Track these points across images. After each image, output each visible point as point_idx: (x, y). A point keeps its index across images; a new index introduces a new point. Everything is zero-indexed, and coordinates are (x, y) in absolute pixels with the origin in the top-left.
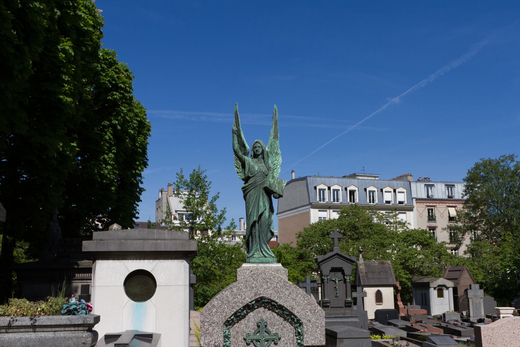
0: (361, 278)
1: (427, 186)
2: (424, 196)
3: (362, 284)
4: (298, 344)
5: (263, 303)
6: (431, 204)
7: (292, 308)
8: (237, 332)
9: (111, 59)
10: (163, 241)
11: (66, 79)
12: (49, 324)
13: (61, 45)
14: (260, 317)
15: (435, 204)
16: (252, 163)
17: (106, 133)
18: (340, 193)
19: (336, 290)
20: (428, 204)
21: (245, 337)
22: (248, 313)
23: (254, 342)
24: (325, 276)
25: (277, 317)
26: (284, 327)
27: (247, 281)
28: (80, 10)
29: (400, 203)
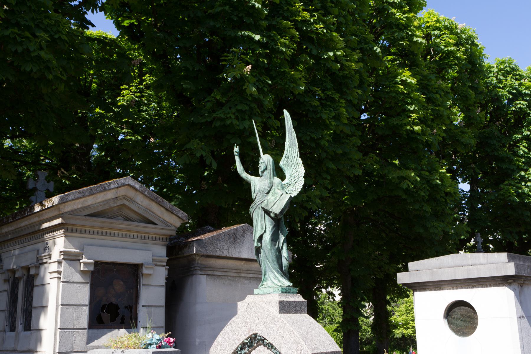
7: (280, 347)
9: (506, 67)
10: (475, 267)
11: (412, 109)
17: (519, 147)
28: (417, 36)
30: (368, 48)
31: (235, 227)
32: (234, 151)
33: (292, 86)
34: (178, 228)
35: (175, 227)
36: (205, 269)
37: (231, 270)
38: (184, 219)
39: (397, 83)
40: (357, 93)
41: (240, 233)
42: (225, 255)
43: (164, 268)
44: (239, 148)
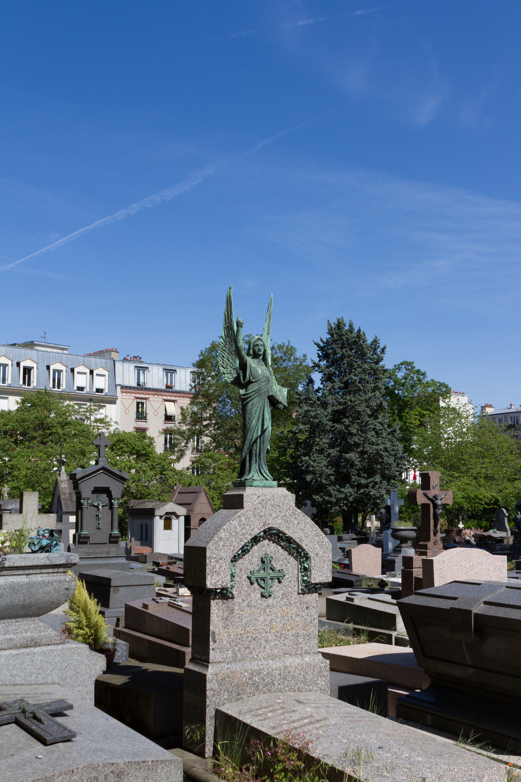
0: (63, 502)
1: (139, 369)
2: (133, 383)
3: (64, 510)
4: (304, 581)
5: (271, 534)
6: (142, 396)
7: (301, 540)
8: (241, 570)
12: (23, 564)
14: (265, 551)
15: (147, 396)
16: (253, 365)
18: (9, 369)
19: (99, 520)
20: (138, 395)
21: (250, 575)
23: (259, 580)
24: (84, 499)
25: (282, 551)
26: (288, 562)
27: (255, 509)
29: (98, 390)
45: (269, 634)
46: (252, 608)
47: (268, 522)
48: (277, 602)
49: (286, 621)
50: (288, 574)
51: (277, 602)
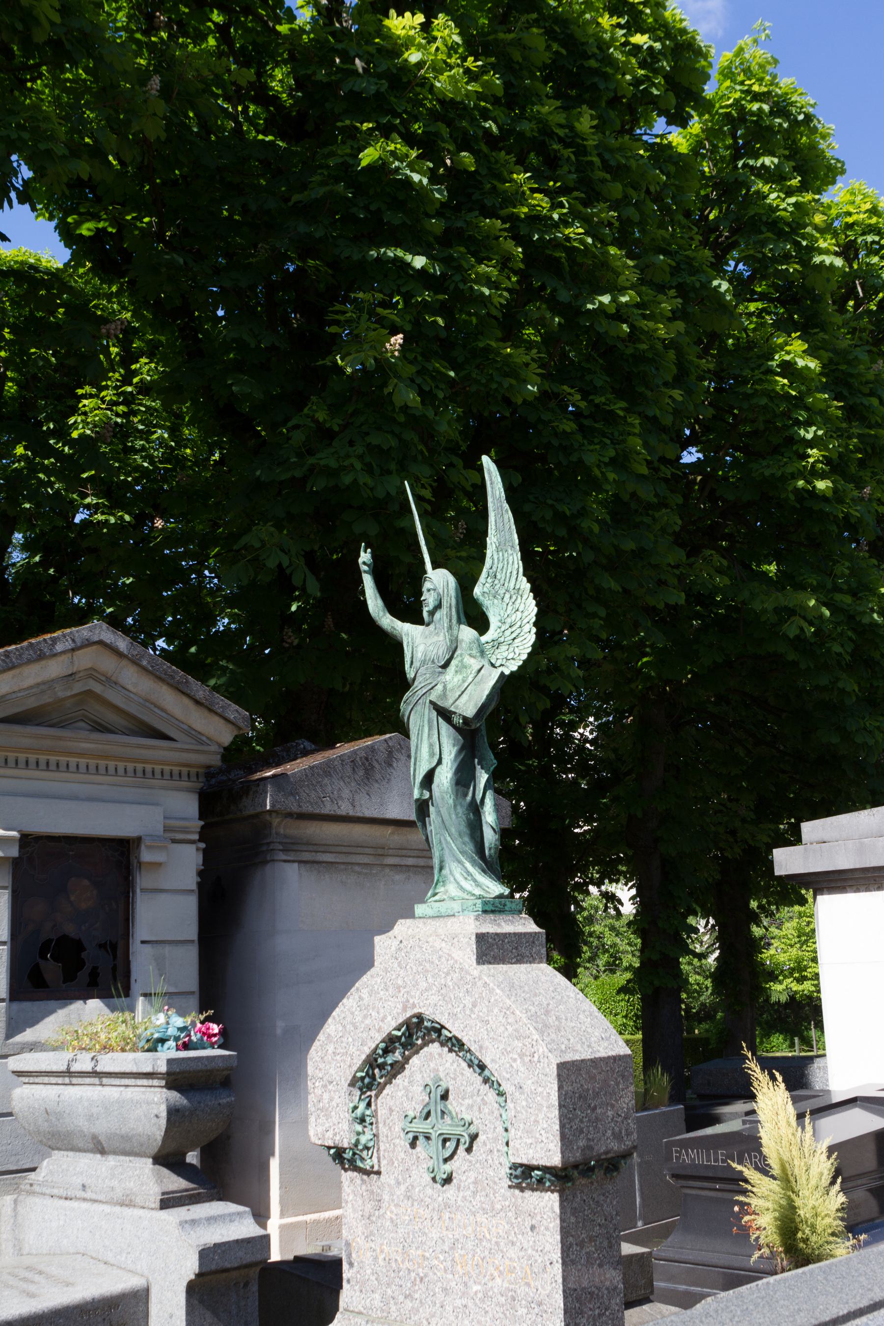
7: (481, 1047)
11: (809, 436)
13: (776, 357)
22: (407, 1060)
28: (821, 251)
30: (698, 285)
31: (368, 742)
32: (360, 561)
33: (506, 385)
34: (225, 749)
35: (219, 744)
36: (295, 847)
37: (359, 850)
38: (242, 725)
39: (770, 371)
40: (670, 397)
41: (382, 756)
42: (344, 813)
43: (194, 847)
44: (372, 553)
45: (450, 1276)
46: (416, 1204)
47: (411, 1001)
48: (464, 1198)
49: (487, 1253)
50: (485, 1132)
51: (464, 1198)
